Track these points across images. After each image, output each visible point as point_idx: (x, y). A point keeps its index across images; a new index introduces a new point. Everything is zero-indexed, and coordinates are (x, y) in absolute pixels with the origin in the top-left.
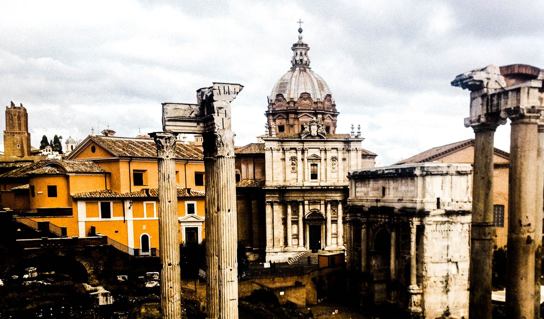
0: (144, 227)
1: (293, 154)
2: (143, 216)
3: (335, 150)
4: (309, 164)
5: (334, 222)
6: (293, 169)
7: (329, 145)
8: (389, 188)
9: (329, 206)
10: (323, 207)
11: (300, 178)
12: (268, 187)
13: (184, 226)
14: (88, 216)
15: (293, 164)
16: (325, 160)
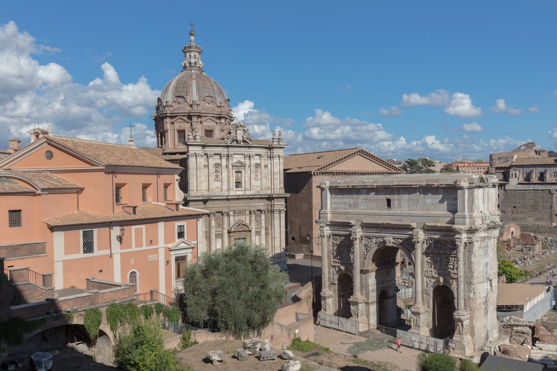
0: (132, 261)
1: (216, 160)
2: (132, 248)
3: (258, 157)
4: (234, 171)
5: (258, 233)
6: (217, 176)
7: (253, 151)
8: (399, 200)
9: (253, 216)
10: (248, 217)
11: (225, 187)
12: (192, 197)
13: (173, 255)
14: (66, 253)
15: (216, 171)
16: (250, 166)
